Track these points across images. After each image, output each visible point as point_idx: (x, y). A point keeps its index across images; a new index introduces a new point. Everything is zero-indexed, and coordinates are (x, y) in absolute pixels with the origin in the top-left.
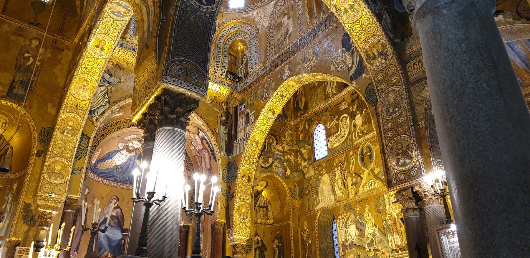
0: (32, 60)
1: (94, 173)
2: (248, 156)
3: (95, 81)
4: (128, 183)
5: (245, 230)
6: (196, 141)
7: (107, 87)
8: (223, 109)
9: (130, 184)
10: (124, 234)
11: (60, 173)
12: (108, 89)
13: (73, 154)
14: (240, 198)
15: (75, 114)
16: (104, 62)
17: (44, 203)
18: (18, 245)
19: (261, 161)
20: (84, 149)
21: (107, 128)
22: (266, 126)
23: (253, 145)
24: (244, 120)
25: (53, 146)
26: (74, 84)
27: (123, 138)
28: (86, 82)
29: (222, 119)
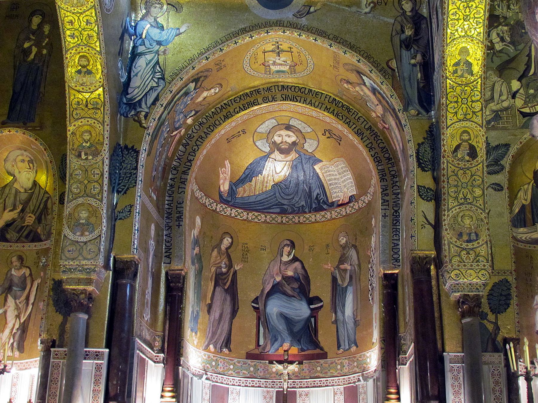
0: (34, 50)
1: (234, 206)
2: (457, 102)
3: (95, 52)
4: (307, 210)
5: (475, 264)
6: (370, 100)
7: (157, 52)
8: (404, 12)
9: (310, 212)
10: (312, 307)
11: (88, 224)
12: (158, 55)
13: (103, 185)
14: (456, 198)
15: (89, 119)
16: (94, 14)
17: (70, 276)
18: (53, 346)
19: (519, 102)
20: (130, 173)
21: (205, 121)
22: (471, 20)
23: (459, 73)
24: (436, 20)
25: (69, 182)
26: (69, 69)
27: (255, 131)
28: (83, 59)
29: (403, 37)
